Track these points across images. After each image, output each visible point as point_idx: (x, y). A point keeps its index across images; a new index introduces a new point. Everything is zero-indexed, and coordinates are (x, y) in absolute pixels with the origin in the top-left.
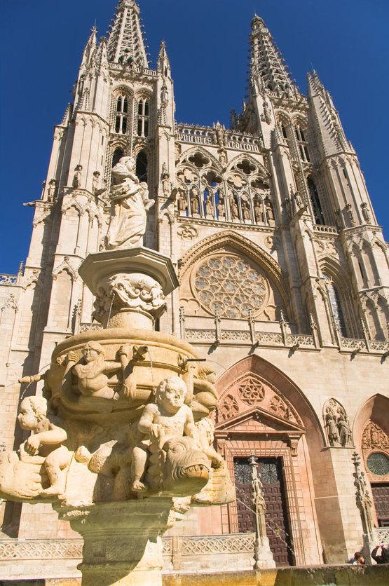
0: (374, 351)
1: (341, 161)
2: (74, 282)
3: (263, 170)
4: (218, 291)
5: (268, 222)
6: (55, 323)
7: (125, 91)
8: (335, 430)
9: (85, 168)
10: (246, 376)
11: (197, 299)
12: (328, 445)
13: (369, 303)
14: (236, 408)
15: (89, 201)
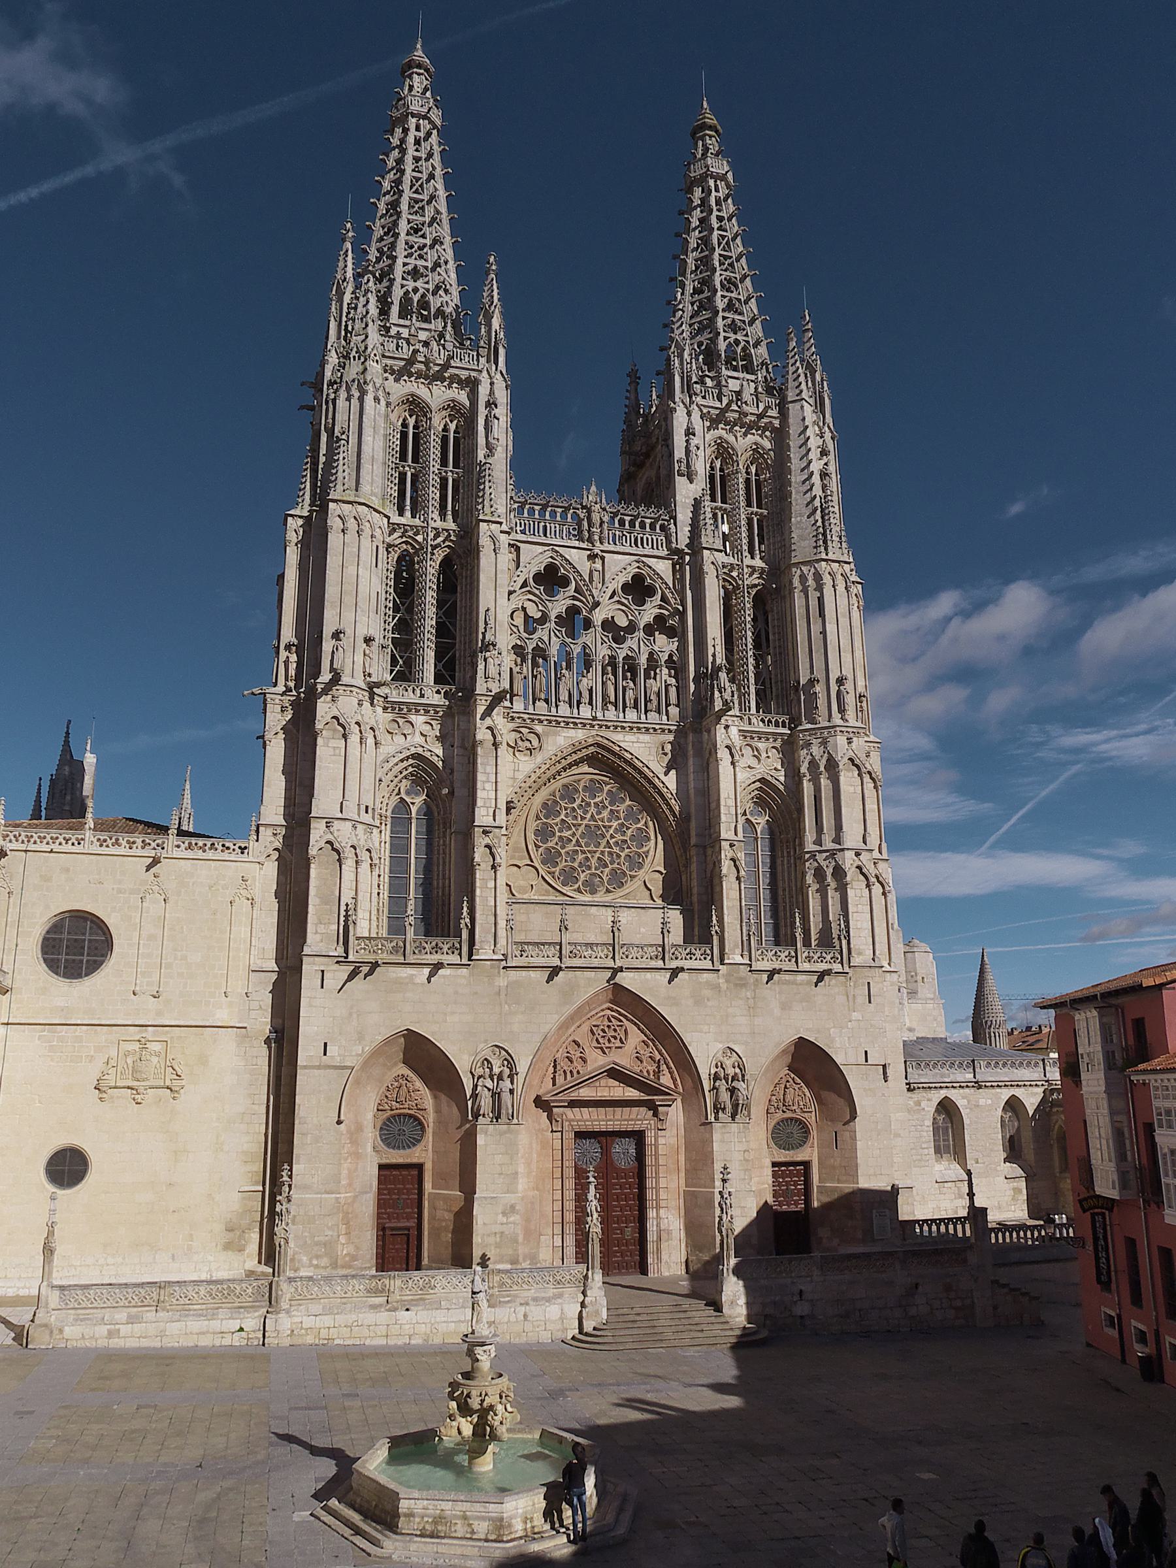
0: (806, 966)
1: (818, 577)
2: (343, 866)
3: (669, 596)
4: (570, 847)
5: (667, 711)
6: (318, 937)
7: (415, 405)
8: (725, 1097)
9: (349, 632)
10: (603, 1010)
11: (536, 865)
12: (711, 1118)
13: (819, 874)
14: (584, 1060)
15: (360, 704)
